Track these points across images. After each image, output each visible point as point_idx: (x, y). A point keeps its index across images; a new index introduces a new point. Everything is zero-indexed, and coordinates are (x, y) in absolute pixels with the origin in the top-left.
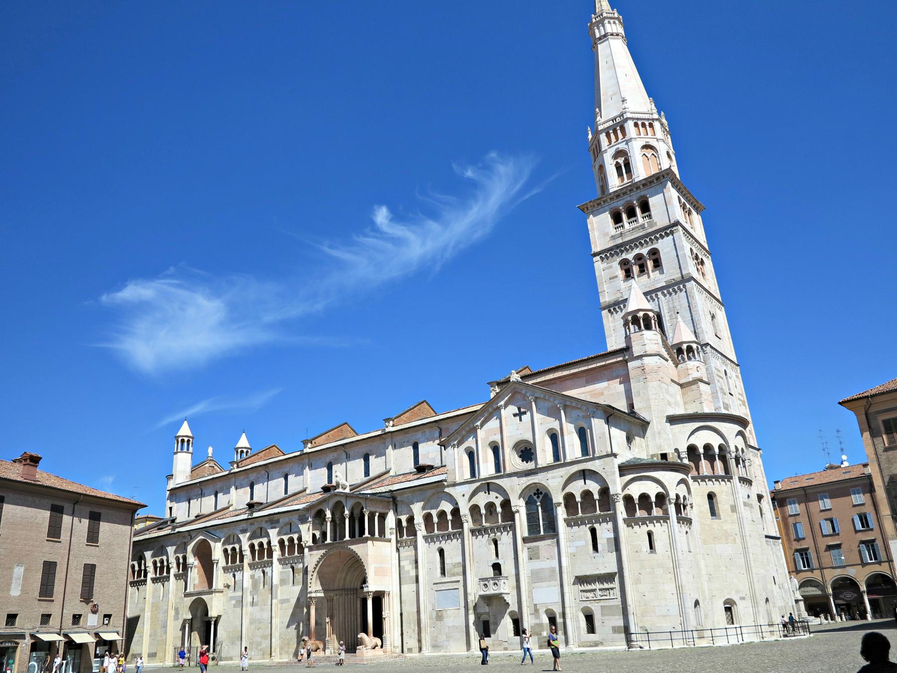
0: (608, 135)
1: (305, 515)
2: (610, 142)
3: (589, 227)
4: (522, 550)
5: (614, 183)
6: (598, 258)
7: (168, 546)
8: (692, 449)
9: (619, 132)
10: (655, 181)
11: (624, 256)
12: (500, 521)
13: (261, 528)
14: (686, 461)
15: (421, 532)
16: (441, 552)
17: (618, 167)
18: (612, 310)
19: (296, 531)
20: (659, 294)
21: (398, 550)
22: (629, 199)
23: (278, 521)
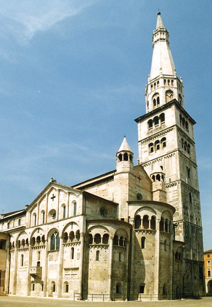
6: (140, 143)
8: (137, 218)
11: (151, 141)
14: (132, 223)
20: (163, 157)
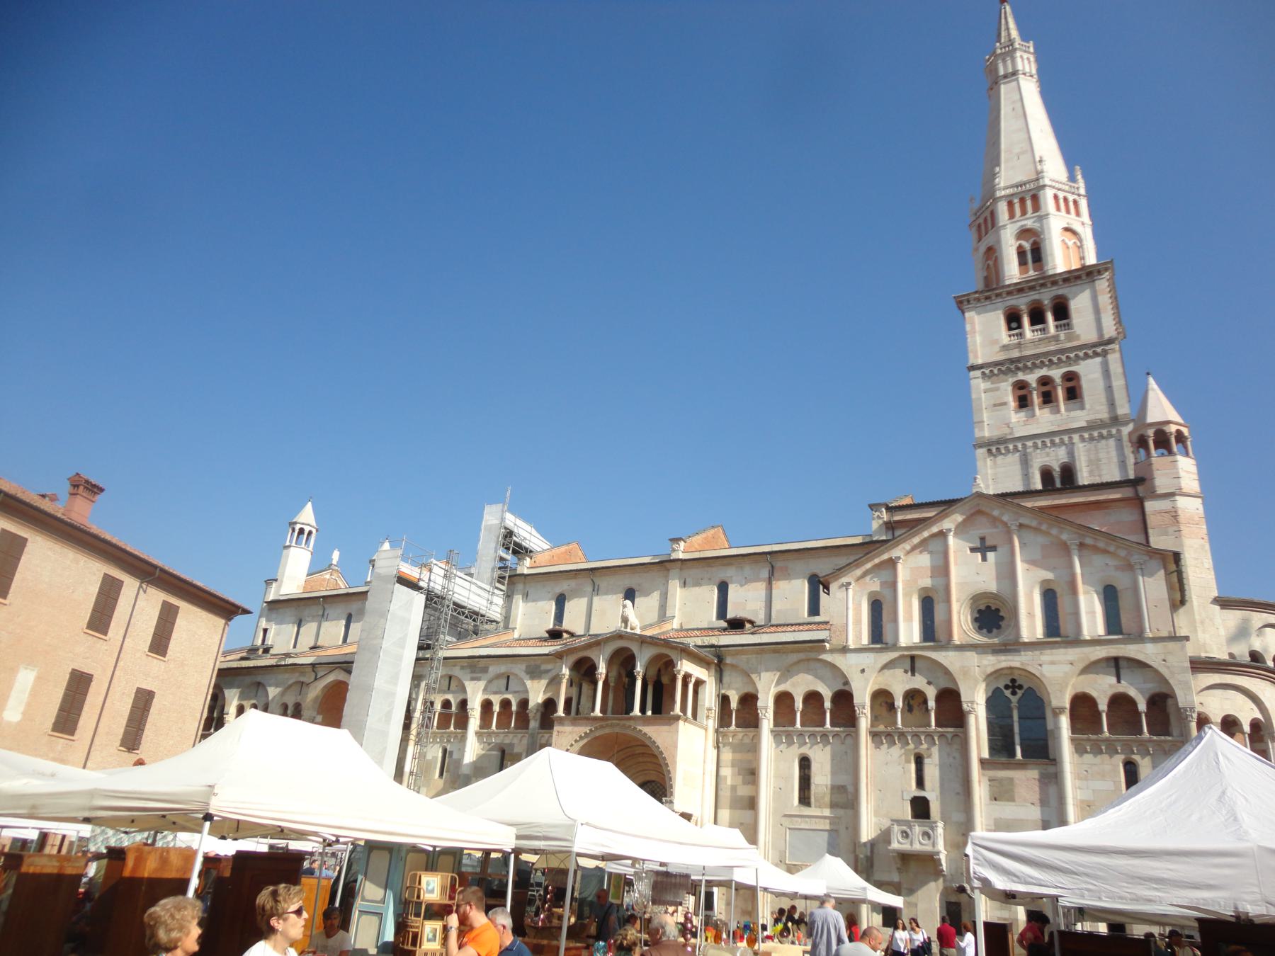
0: (1010, 204)
1: (539, 666)
2: (1012, 215)
3: (968, 327)
4: (979, 781)
5: (1012, 271)
6: (978, 373)
7: (270, 686)
9: (1029, 203)
10: (1084, 277)
11: (1021, 376)
12: (933, 723)
13: (450, 678)
15: (767, 723)
16: (805, 763)
17: (1021, 253)
18: (994, 450)
19: (517, 689)
20: (1076, 437)
21: (718, 747)
22: (1036, 297)
23: (485, 670)
